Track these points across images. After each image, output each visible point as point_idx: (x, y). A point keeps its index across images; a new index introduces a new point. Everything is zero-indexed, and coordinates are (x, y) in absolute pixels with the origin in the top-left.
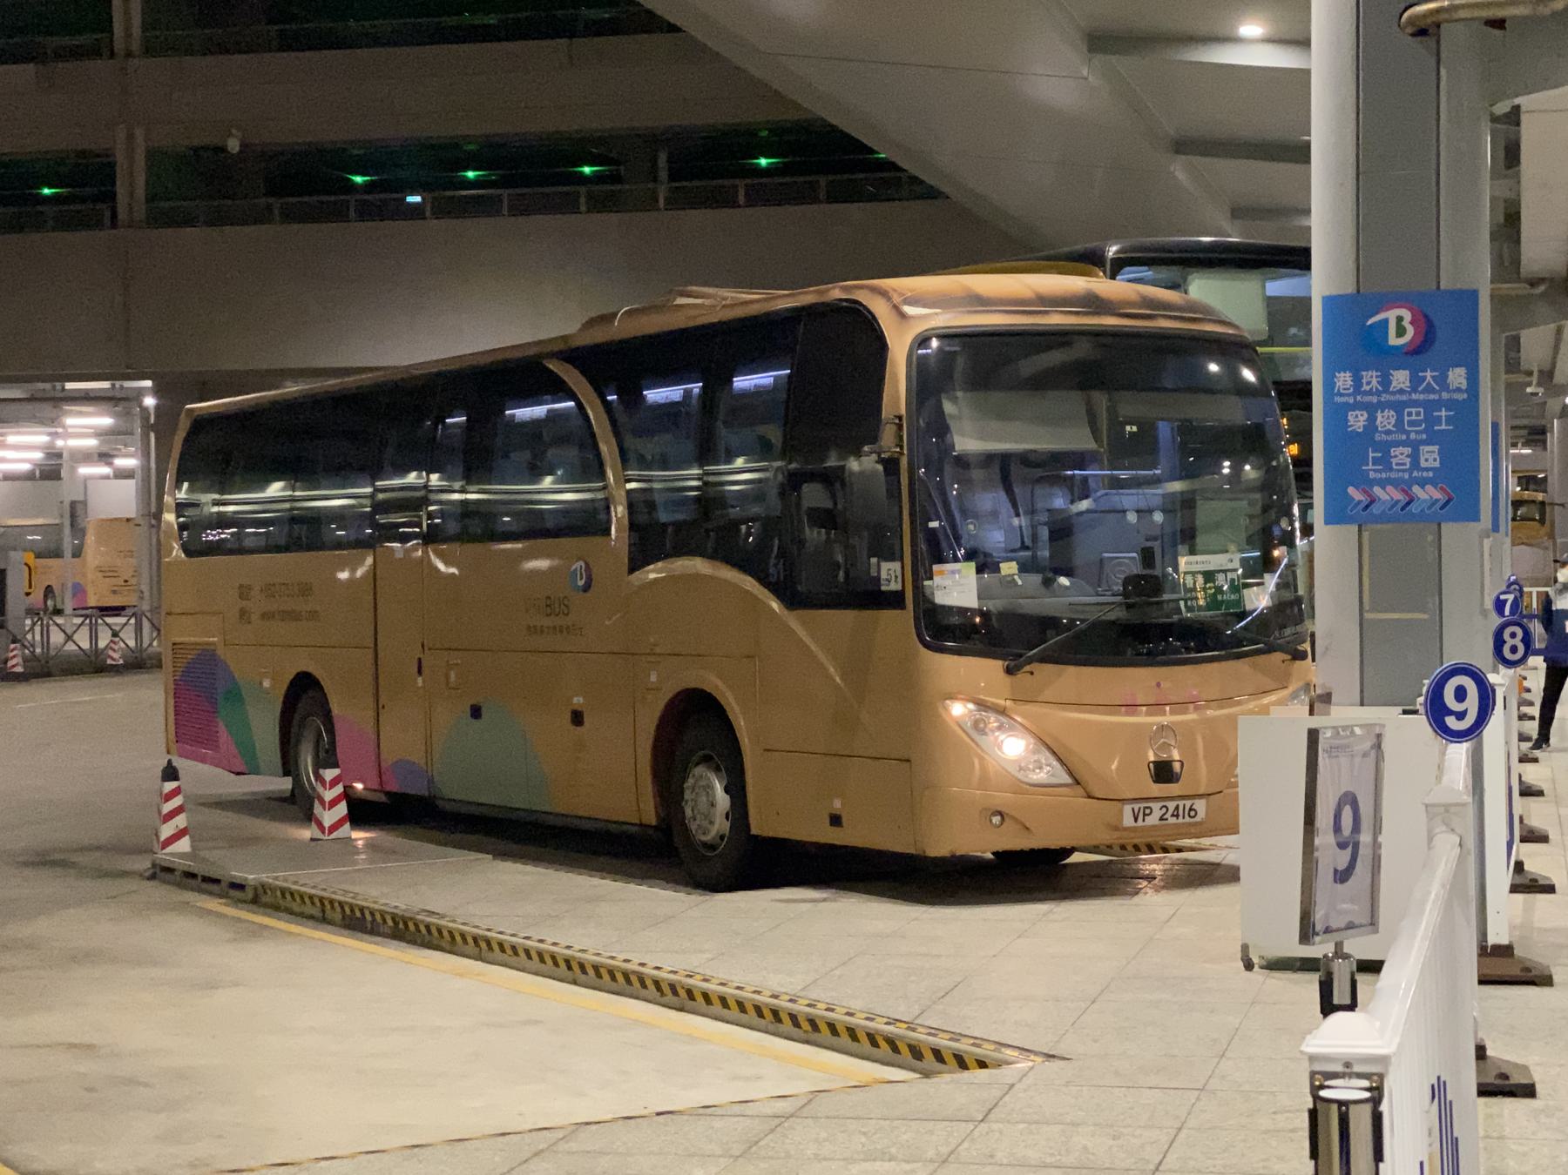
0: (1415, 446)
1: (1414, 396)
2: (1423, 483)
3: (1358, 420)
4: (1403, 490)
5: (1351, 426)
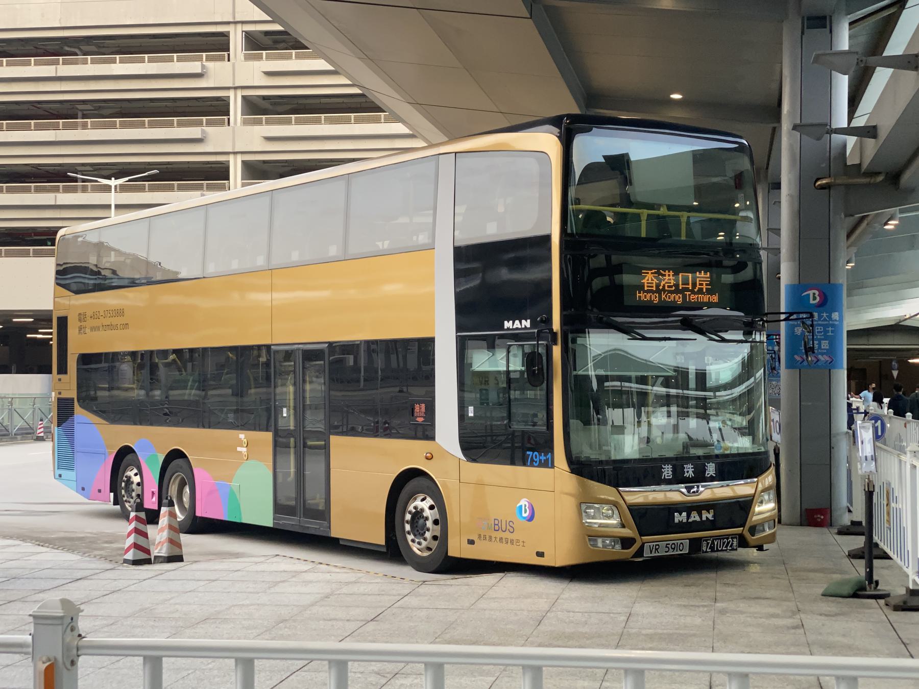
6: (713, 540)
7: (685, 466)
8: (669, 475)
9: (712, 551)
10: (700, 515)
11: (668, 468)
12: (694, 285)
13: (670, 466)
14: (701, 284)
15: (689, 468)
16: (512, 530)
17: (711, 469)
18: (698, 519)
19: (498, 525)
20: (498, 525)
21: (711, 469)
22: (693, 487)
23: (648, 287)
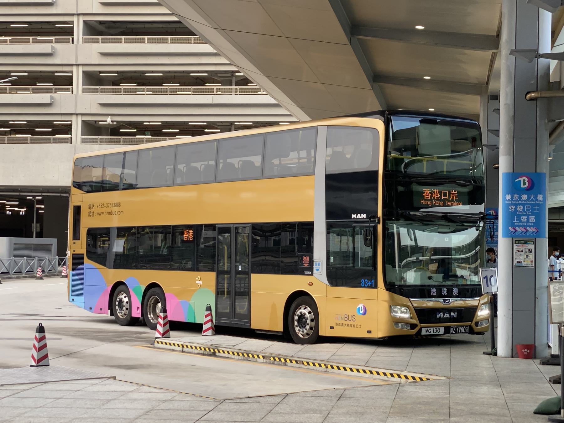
0: (528, 216)
1: (528, 202)
2: (530, 226)
3: (512, 208)
4: (524, 228)
5: (510, 210)
6: (456, 327)
9: (456, 333)
10: (450, 315)
13: (435, 289)
14: (453, 197)
16: (354, 320)
17: (456, 291)
18: (449, 317)
19: (346, 317)
20: (346, 317)
21: (456, 291)
22: (447, 300)
23: (426, 197)
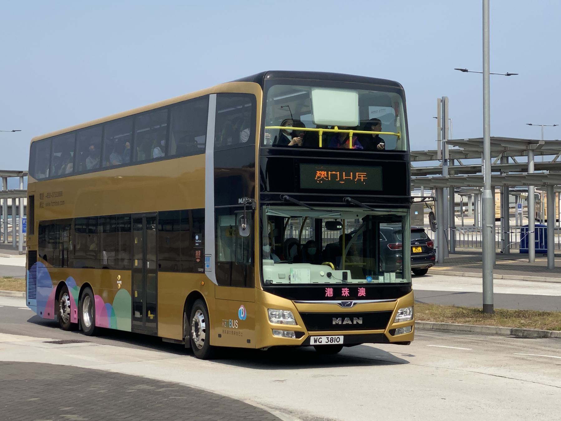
7: (342, 289)
8: (331, 294)
10: (352, 322)
11: (330, 290)
12: (354, 177)
15: (346, 291)
17: (362, 292)
21: (362, 292)
